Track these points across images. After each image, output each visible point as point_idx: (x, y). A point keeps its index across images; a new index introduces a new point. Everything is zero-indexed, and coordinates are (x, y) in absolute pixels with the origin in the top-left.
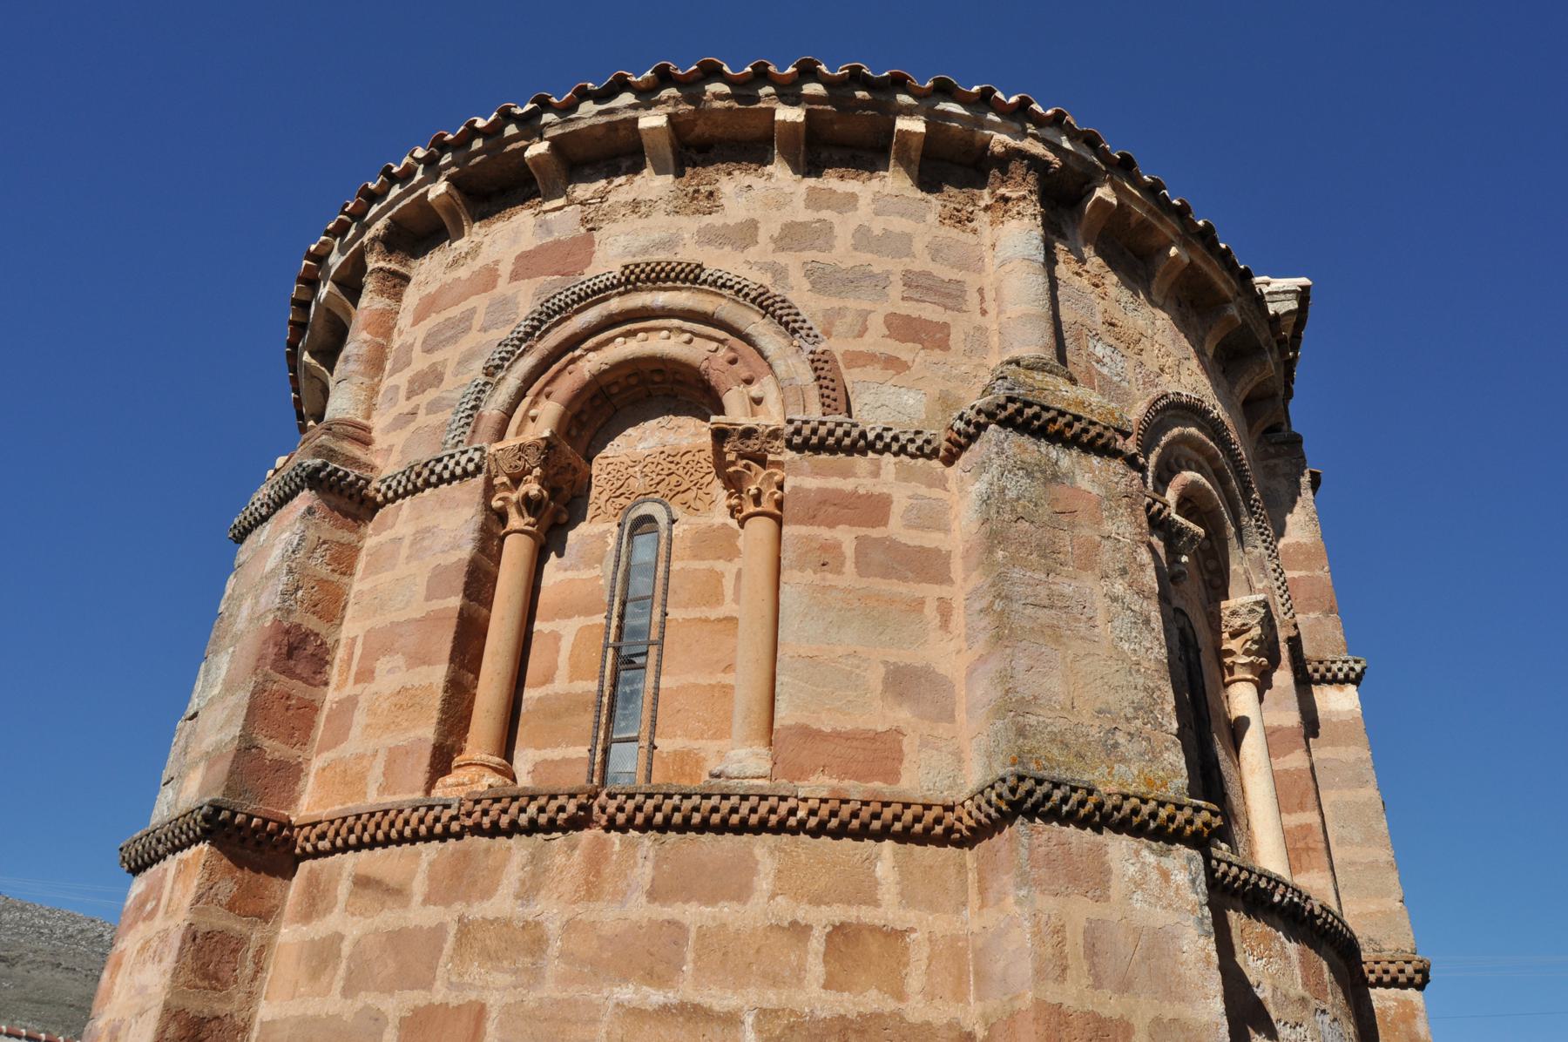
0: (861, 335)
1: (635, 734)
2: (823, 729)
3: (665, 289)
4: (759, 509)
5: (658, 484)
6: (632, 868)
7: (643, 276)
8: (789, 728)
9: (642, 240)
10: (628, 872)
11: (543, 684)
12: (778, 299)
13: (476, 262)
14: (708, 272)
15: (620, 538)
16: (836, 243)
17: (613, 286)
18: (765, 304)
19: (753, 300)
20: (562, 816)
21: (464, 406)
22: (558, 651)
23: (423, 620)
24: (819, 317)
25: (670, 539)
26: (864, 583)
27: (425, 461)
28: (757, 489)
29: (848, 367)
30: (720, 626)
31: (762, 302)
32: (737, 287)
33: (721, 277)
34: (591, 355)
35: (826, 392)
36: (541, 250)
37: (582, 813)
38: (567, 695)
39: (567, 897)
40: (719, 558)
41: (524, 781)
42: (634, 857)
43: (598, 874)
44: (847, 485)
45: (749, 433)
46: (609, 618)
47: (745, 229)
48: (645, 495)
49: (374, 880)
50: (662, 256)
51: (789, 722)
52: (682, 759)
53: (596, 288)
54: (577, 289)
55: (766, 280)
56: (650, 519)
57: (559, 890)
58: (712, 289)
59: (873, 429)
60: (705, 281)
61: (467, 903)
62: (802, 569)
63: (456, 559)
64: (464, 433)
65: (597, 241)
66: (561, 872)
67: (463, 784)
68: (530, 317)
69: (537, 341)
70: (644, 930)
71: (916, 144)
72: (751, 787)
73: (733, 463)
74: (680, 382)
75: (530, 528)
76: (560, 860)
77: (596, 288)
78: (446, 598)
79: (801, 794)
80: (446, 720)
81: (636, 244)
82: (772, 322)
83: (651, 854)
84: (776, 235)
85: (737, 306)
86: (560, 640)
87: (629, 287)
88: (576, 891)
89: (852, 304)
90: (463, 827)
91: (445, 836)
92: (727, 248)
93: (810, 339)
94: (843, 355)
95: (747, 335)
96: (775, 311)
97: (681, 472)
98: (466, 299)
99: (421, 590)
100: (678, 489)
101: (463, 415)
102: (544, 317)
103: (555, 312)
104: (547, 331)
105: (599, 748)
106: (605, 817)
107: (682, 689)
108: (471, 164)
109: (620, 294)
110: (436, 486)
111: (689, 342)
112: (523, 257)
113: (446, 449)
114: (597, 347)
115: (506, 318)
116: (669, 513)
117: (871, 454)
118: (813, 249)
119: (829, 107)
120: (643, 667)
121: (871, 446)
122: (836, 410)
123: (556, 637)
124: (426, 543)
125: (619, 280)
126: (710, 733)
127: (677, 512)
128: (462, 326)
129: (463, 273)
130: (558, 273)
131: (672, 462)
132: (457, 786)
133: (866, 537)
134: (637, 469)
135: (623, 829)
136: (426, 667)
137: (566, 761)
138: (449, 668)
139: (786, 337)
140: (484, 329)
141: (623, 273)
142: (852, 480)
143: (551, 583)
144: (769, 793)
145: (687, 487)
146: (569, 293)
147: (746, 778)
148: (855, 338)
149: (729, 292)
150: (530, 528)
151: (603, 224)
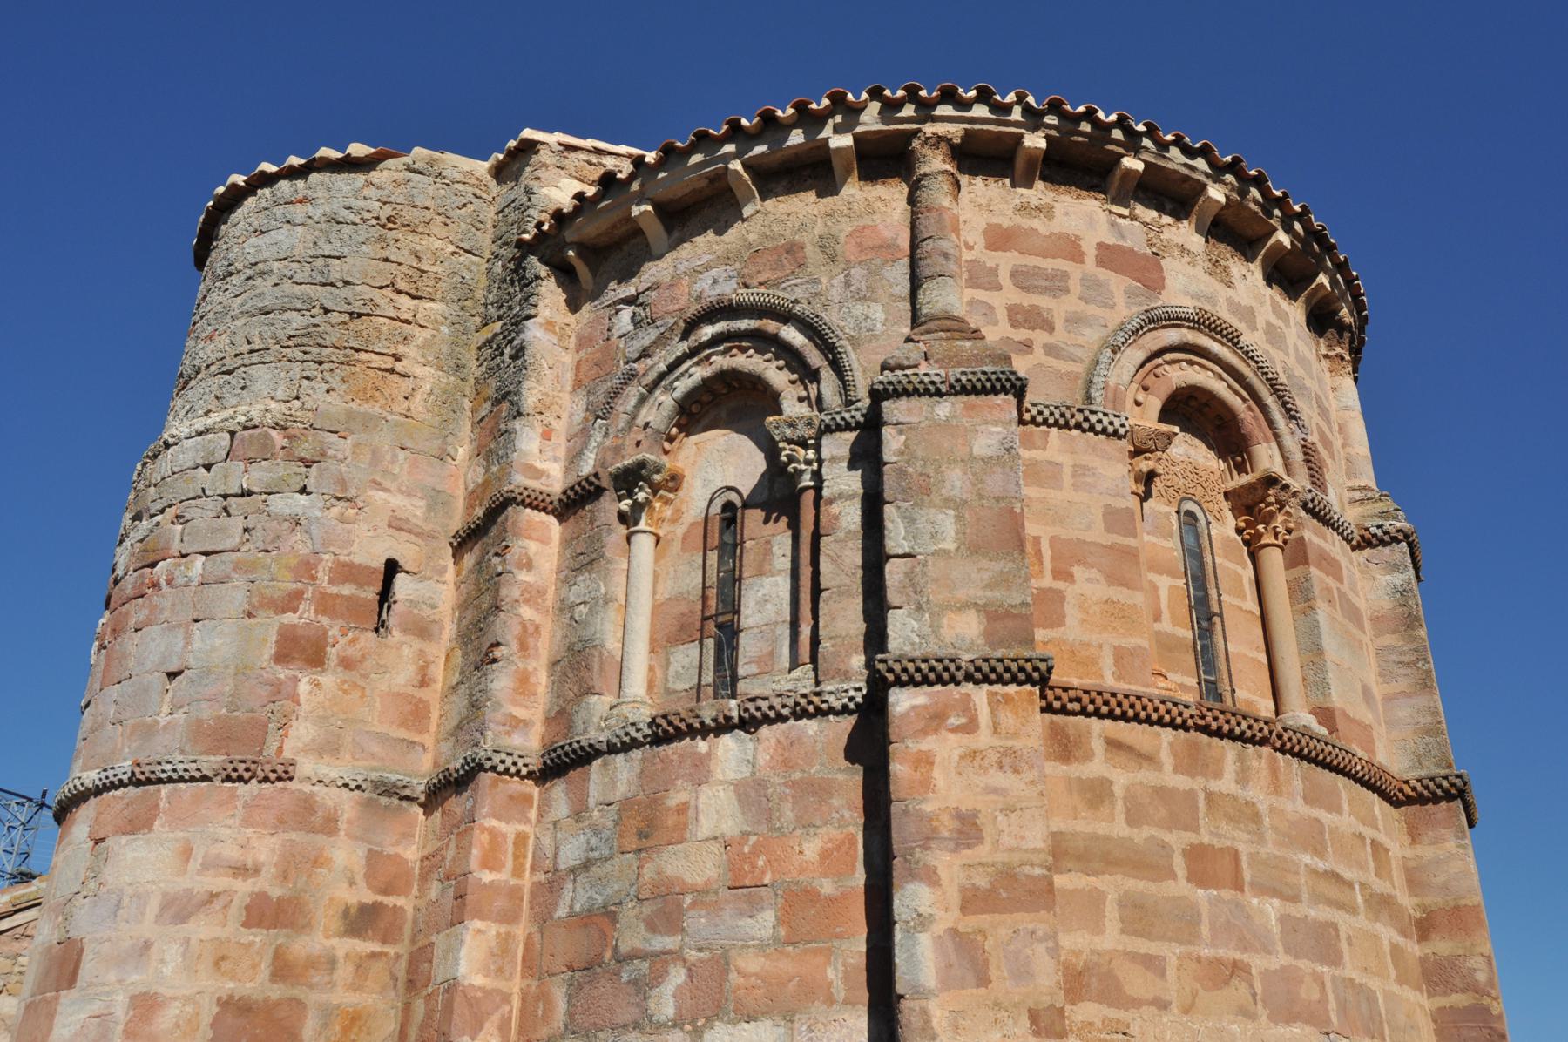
3: (1215, 339)
17: (1188, 320)
19: (1268, 380)
20: (1259, 735)
22: (1158, 598)
43: (1277, 778)
45: (1286, 487)
60: (1242, 348)
71: (1321, 294)
73: (1271, 504)
76: (1255, 763)
91: (1184, 727)
108: (1073, 138)
109: (1189, 328)
110: (1084, 431)
121: (1332, 526)
124: (1089, 480)
130: (1139, 281)
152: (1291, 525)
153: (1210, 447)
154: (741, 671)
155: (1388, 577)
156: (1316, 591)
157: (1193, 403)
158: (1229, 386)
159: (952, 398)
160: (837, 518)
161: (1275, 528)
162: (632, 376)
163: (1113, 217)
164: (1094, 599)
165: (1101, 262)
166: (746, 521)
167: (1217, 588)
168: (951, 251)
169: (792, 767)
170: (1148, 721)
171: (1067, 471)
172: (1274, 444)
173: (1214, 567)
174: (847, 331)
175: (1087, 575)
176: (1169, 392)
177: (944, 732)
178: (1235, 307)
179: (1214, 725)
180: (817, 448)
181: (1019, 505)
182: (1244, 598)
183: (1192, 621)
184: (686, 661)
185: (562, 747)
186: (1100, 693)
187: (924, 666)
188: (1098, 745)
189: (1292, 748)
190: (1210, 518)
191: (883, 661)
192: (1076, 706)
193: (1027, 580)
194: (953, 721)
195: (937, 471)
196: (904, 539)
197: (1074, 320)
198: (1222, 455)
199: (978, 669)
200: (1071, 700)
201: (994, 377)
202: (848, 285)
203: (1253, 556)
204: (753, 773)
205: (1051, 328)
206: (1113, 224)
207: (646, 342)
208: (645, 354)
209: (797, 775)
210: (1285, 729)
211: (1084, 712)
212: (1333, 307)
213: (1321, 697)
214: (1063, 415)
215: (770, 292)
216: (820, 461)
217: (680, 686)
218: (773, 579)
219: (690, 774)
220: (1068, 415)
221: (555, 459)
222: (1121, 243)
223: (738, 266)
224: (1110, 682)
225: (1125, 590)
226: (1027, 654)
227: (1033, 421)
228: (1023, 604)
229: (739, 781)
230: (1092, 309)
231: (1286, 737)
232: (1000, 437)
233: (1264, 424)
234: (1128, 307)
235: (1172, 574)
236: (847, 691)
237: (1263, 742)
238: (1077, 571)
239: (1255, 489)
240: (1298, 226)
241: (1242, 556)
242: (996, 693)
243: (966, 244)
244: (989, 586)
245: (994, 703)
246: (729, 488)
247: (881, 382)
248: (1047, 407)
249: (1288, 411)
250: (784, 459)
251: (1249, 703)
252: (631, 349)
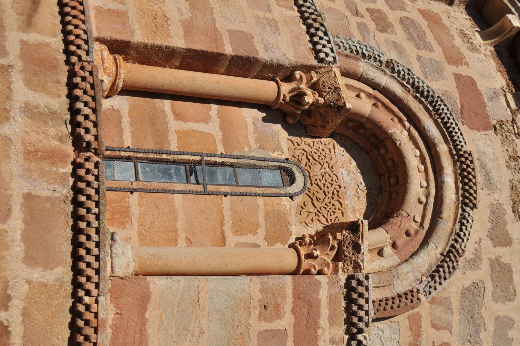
0: (434, 326)
1: (141, 179)
2: (148, 312)
3: (456, 183)
4: (303, 258)
5: (318, 185)
6: (47, 182)
7: (465, 166)
8: (148, 288)
9: (490, 165)
10: (45, 179)
11: (174, 113)
12: (455, 264)
13: (466, 49)
14: (471, 212)
15: (278, 161)
16: (499, 304)
17: (456, 146)
18: (451, 255)
19: (453, 246)
20: (83, 132)
21: (364, 48)
22: (197, 122)
23: (216, 30)
24: (445, 295)
25: (279, 196)
26: (254, 337)
27: (325, 24)
28: (318, 256)
29: (409, 317)
30: (219, 234)
31: (452, 253)
32: (462, 234)
33: (468, 222)
34: (406, 133)
35: (390, 303)
36: (478, 94)
37: (84, 145)
38: (167, 130)
39: (27, 137)
40: (267, 231)
41: (106, 104)
42: (55, 183)
43: (43, 158)
44: (324, 321)
45: (357, 248)
46: (221, 155)
47: (504, 237)
48: (309, 176)
49: (37, 7)
50: (480, 178)
51: (152, 287)
52: (123, 212)
53: (454, 134)
54: (451, 121)
55: (468, 255)
56: (292, 180)
57: (32, 132)
58: (459, 216)
59: (365, 338)
60: (464, 211)
61: (22, 70)
62: (261, 291)
63: (258, 49)
64: (346, 49)
65: (487, 133)
66: (44, 133)
67: (103, 63)
68: (430, 90)
69: (413, 95)
70: (4, 192)
72: (105, 263)
73: (335, 238)
74: (391, 196)
75: (282, 98)
76: (52, 131)
77: (454, 134)
78: (231, 44)
79: (100, 299)
80: (147, 49)
81: (487, 160)
82: (438, 260)
83: (57, 195)
84: (502, 260)
85: (448, 234)
86: (205, 123)
87: (456, 157)
88: (31, 143)
89: (456, 318)
90: (74, 64)
92: (489, 226)
93: (427, 289)
94: (418, 313)
95: (428, 243)
96: (446, 262)
97: (327, 200)
98: (440, 45)
99: (235, 27)
100: (314, 199)
101: (358, 48)
102: (430, 99)
103: (434, 107)
104: (421, 102)
105: (131, 154)
106: (82, 161)
107: (173, 210)
109: (450, 151)
110: (308, 32)
111: (420, 202)
112: (472, 82)
113: (334, 38)
114: (411, 137)
115: (428, 73)
116: (297, 194)
117: (346, 337)
118: (494, 288)
120: (188, 182)
122: (378, 310)
123: (207, 120)
124: (268, 28)
125: (460, 150)
126: (143, 231)
127: (299, 199)
128: (420, 43)
129: (458, 41)
130: (462, 106)
131: (333, 194)
132: (102, 59)
133: (286, 337)
134: (327, 169)
135: (74, 174)
136: (182, 33)
137: (121, 131)
138: (183, 49)
139: (428, 271)
140: (419, 58)
141: (465, 152)
142: (327, 324)
143: (244, 115)
144: (101, 276)
145: (316, 205)
146: (449, 115)
147: (112, 259)
148: (431, 321)
149: (458, 228)
150: (282, 98)
151: (499, 136)
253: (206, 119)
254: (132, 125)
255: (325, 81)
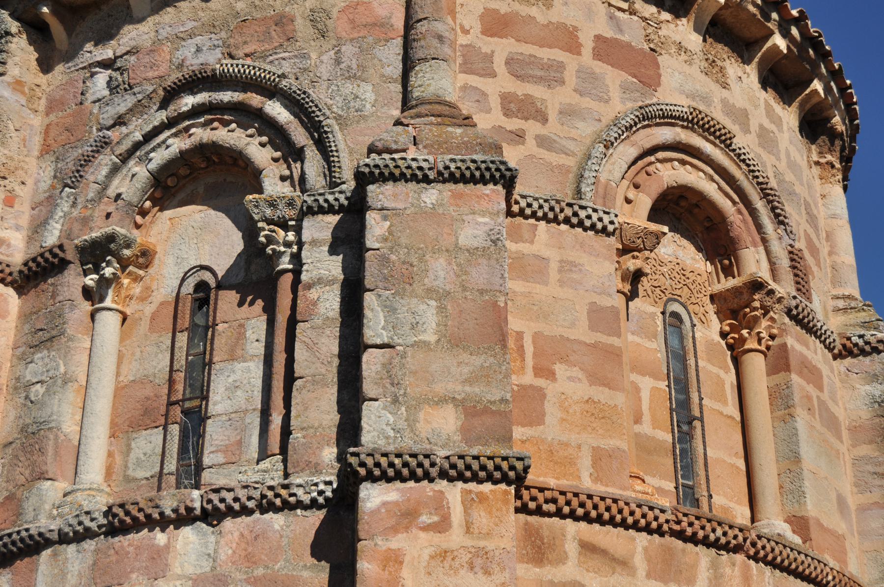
1: (691, 483)
3: (708, 140)
4: (759, 347)
17: (682, 119)
18: (768, 191)
19: (759, 183)
20: (734, 542)
22: (640, 399)
31: (766, 189)
32: (752, 168)
33: (744, 154)
42: (764, 581)
45: (771, 292)
48: (673, 294)
53: (674, 114)
58: (735, 158)
60: (734, 150)
66: (731, 579)
67: (647, 494)
71: (815, 100)
73: (755, 309)
76: (728, 571)
81: (687, 87)
82: (766, 206)
83: (771, 582)
87: (690, 125)
91: (660, 532)
93: (792, 236)
103: (648, 119)
109: (683, 127)
110: (573, 226)
119: (795, 50)
121: (815, 333)
124: (575, 276)
130: (635, 76)
132: (643, 493)
152: (775, 331)
153: (699, 249)
154: (207, 460)
155: (868, 387)
156: (797, 397)
157: (683, 203)
158: (720, 188)
159: (440, 186)
160: (315, 303)
161: (759, 333)
162: (105, 143)
163: (612, 10)
164: (575, 398)
165: (598, 55)
166: (220, 303)
167: (699, 391)
168: (447, 34)
169: (255, 563)
170: (624, 524)
171: (554, 266)
172: (761, 249)
173: (697, 370)
174: (335, 110)
175: (568, 374)
176: (660, 191)
177: (414, 530)
178: (729, 109)
179: (689, 531)
180: (298, 230)
181: (503, 299)
182: (725, 403)
183: (672, 425)
184: (148, 448)
185: (10, 535)
186: (576, 495)
187: (397, 461)
188: (571, 548)
189: (766, 556)
190: (695, 321)
191: (356, 455)
192: (552, 508)
193: (507, 376)
194: (425, 519)
195: (421, 259)
196: (384, 328)
197: (568, 113)
198: (710, 257)
199: (453, 466)
200: (547, 501)
201: (483, 166)
202: (338, 62)
203: (737, 361)
204: (213, 568)
205: (544, 120)
206: (612, 17)
207: (122, 108)
208: (120, 121)
209: (260, 571)
210: (759, 537)
211: (559, 514)
212: (825, 114)
213: (796, 505)
214: (552, 209)
215: (256, 64)
216: (300, 244)
217: (141, 474)
218: (245, 364)
219: (146, 568)
220: (557, 210)
221: (18, 228)
222: (619, 36)
223: (223, 35)
224: (587, 483)
225: (607, 390)
226: (504, 452)
227: (521, 213)
228: (503, 401)
229: (199, 576)
230: (587, 102)
231: (760, 544)
232: (487, 228)
233: (753, 228)
234: (623, 103)
235: (655, 376)
236: (316, 485)
237: (737, 549)
238: (560, 369)
239: (741, 293)
240: (794, 31)
241: (726, 361)
242: (471, 491)
243: (462, 27)
244: (468, 381)
245: (468, 502)
246: (203, 268)
247: (367, 165)
248: (536, 199)
249: (777, 216)
250: (262, 239)
251: (726, 510)
252: (105, 116)
253: (636, 389)
254: (654, 476)
255: (628, 238)
